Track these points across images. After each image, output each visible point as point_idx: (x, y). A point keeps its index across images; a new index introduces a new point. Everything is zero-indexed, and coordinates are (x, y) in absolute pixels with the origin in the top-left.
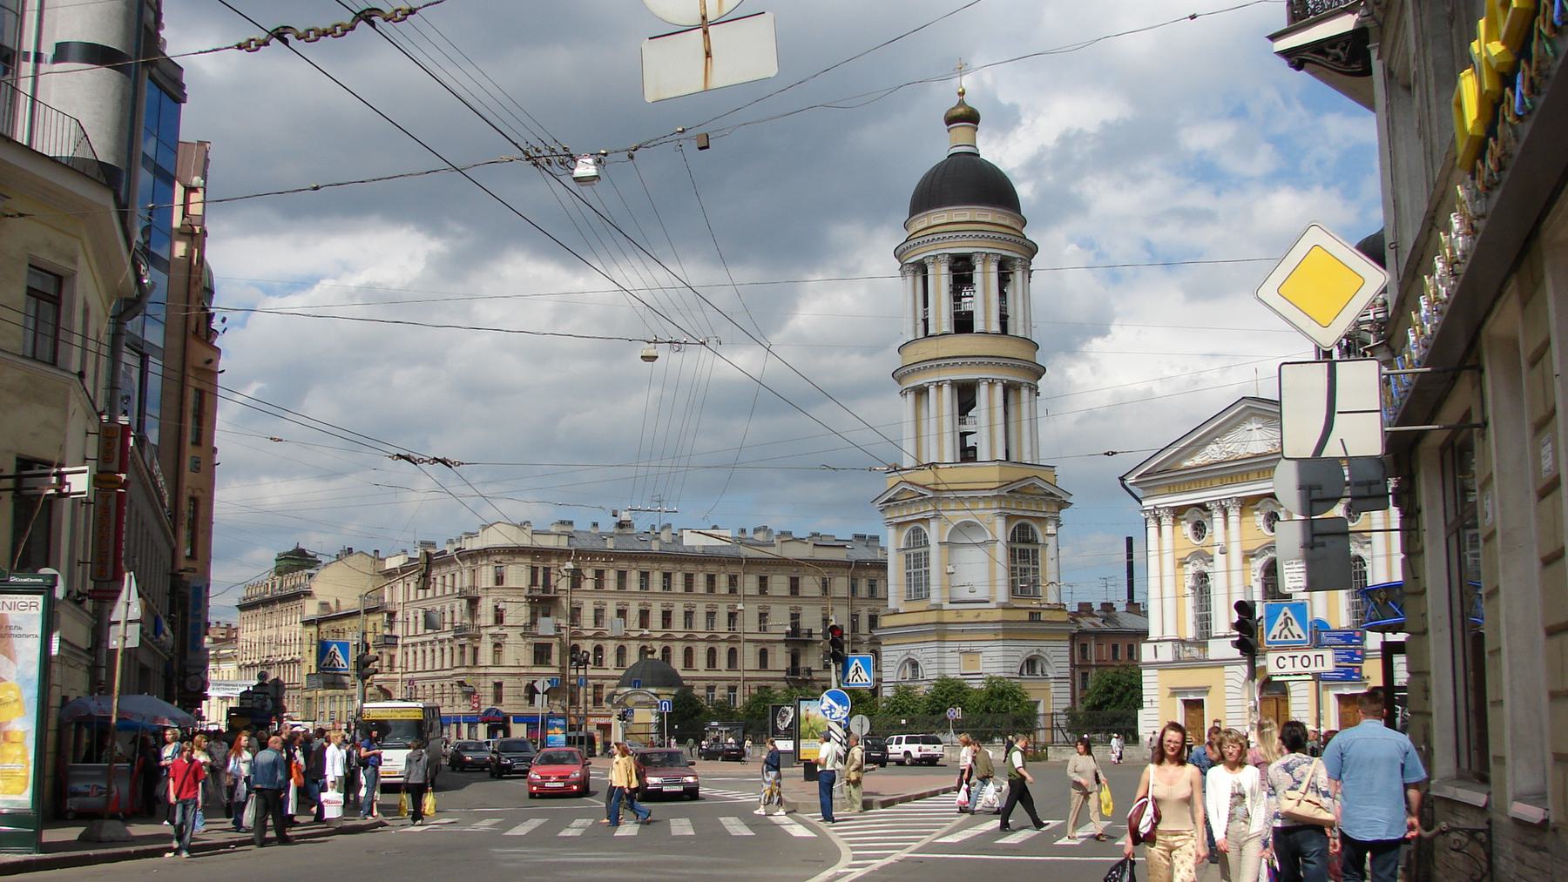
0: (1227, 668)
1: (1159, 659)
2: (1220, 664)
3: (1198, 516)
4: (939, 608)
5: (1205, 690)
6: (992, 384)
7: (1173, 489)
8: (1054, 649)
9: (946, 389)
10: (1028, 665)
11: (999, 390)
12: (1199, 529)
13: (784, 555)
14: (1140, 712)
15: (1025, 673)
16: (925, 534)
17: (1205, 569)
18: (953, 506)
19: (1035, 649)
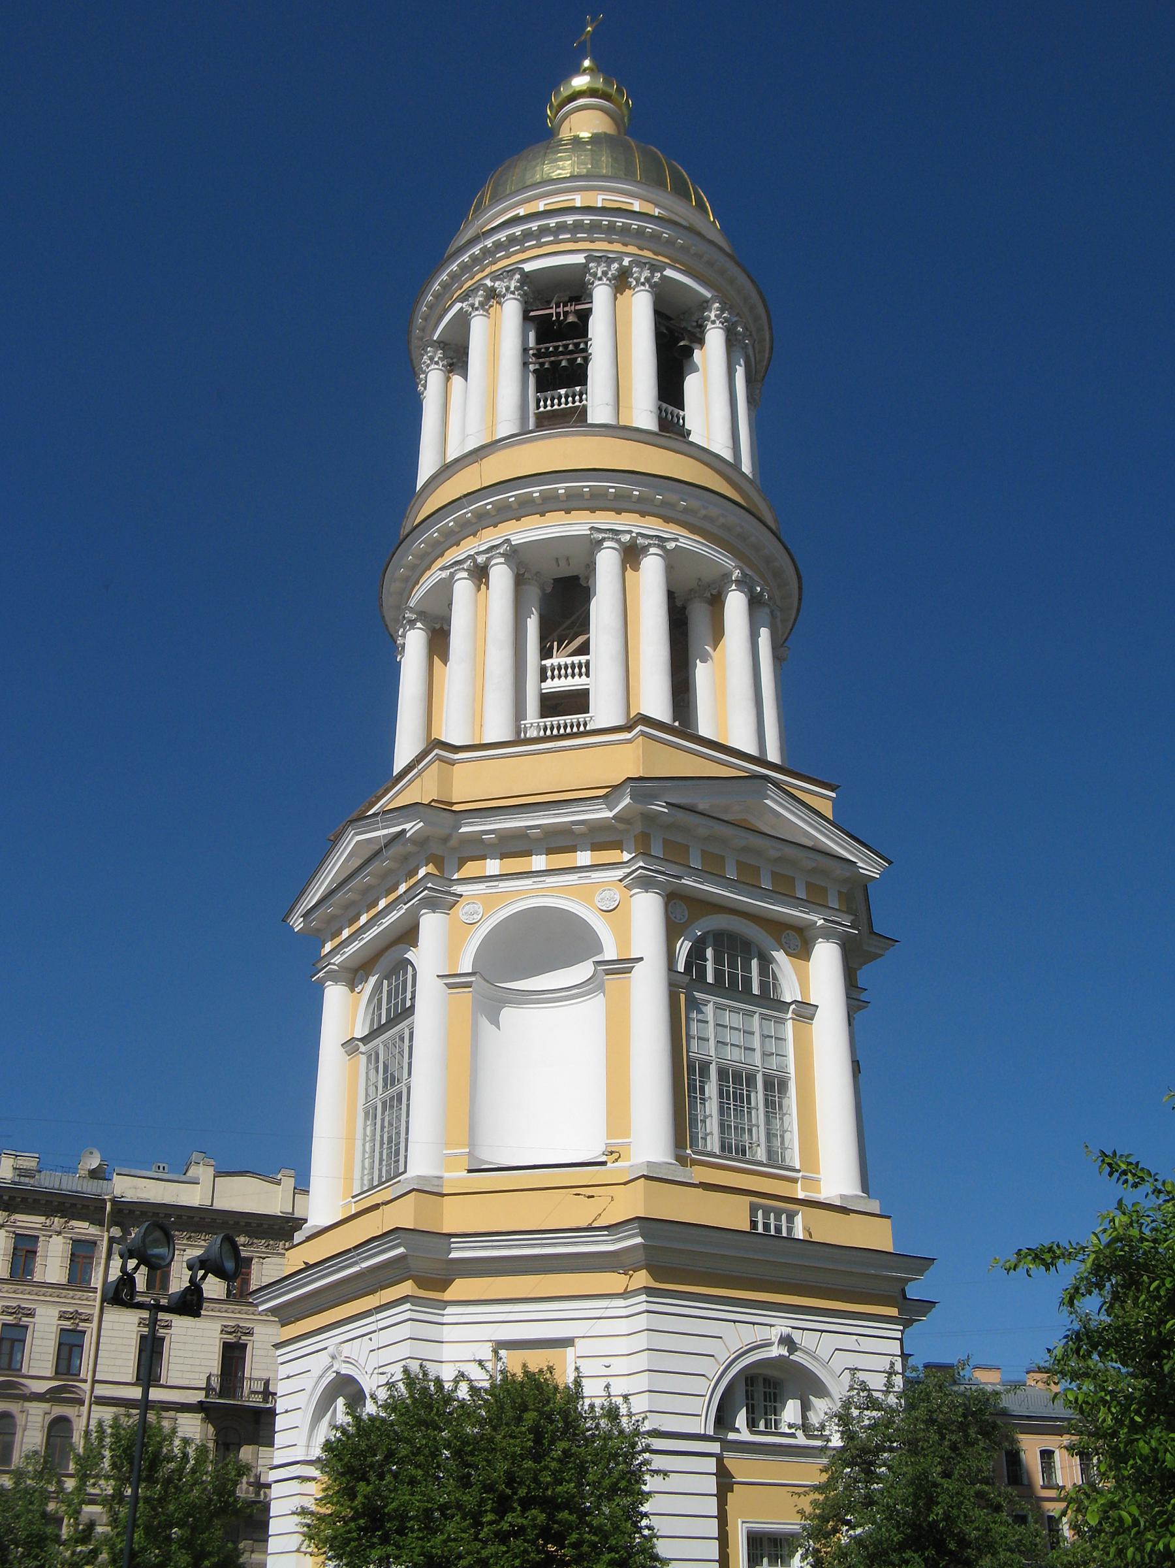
4: (430, 1191)
6: (632, 555)
8: (849, 1342)
9: (501, 576)
10: (749, 1396)
11: (652, 567)
13: (219, 1205)
15: (741, 1420)
18: (493, 866)
19: (774, 1334)
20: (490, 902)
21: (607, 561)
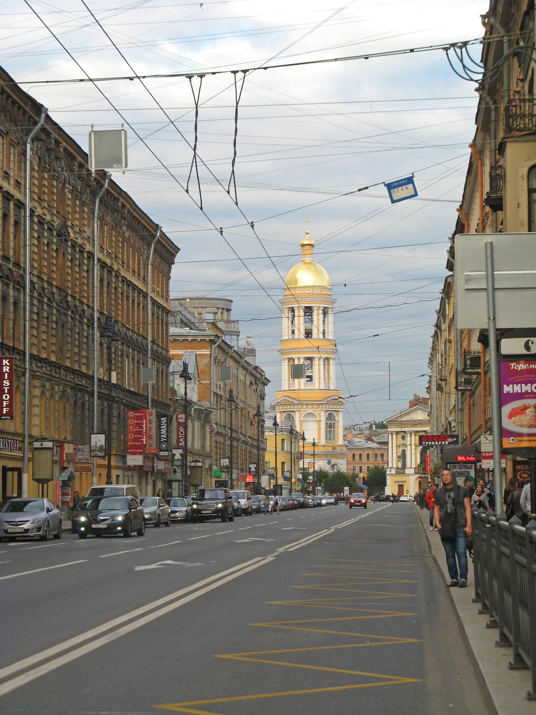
0: (410, 476)
1: (391, 473)
2: (409, 475)
3: (403, 434)
5: (404, 482)
6: (319, 359)
7: (396, 426)
12: (403, 438)
14: (386, 487)
16: (293, 417)
17: (405, 449)
20: (304, 411)
21: (317, 360)
